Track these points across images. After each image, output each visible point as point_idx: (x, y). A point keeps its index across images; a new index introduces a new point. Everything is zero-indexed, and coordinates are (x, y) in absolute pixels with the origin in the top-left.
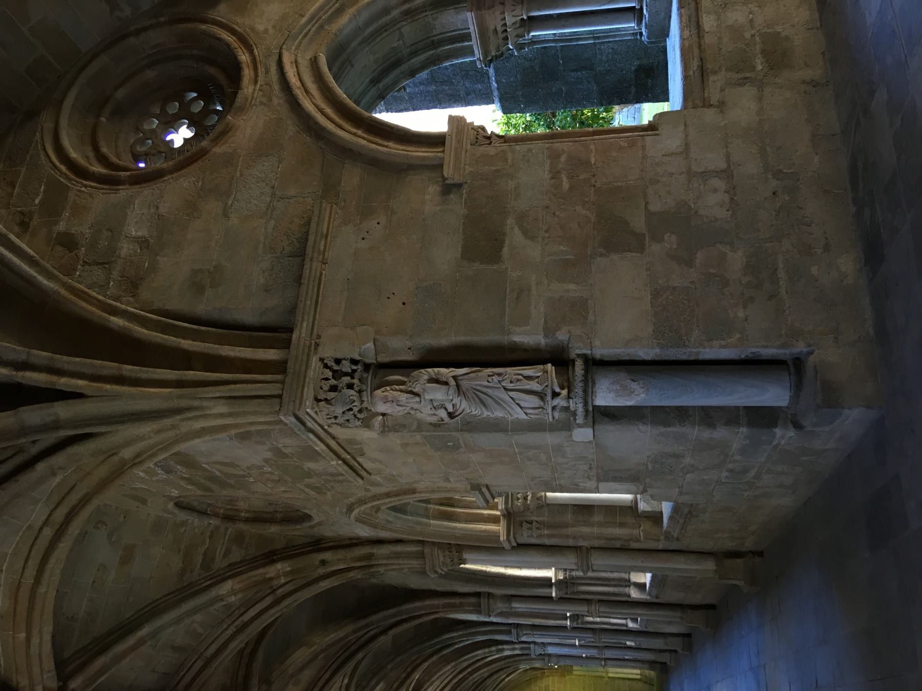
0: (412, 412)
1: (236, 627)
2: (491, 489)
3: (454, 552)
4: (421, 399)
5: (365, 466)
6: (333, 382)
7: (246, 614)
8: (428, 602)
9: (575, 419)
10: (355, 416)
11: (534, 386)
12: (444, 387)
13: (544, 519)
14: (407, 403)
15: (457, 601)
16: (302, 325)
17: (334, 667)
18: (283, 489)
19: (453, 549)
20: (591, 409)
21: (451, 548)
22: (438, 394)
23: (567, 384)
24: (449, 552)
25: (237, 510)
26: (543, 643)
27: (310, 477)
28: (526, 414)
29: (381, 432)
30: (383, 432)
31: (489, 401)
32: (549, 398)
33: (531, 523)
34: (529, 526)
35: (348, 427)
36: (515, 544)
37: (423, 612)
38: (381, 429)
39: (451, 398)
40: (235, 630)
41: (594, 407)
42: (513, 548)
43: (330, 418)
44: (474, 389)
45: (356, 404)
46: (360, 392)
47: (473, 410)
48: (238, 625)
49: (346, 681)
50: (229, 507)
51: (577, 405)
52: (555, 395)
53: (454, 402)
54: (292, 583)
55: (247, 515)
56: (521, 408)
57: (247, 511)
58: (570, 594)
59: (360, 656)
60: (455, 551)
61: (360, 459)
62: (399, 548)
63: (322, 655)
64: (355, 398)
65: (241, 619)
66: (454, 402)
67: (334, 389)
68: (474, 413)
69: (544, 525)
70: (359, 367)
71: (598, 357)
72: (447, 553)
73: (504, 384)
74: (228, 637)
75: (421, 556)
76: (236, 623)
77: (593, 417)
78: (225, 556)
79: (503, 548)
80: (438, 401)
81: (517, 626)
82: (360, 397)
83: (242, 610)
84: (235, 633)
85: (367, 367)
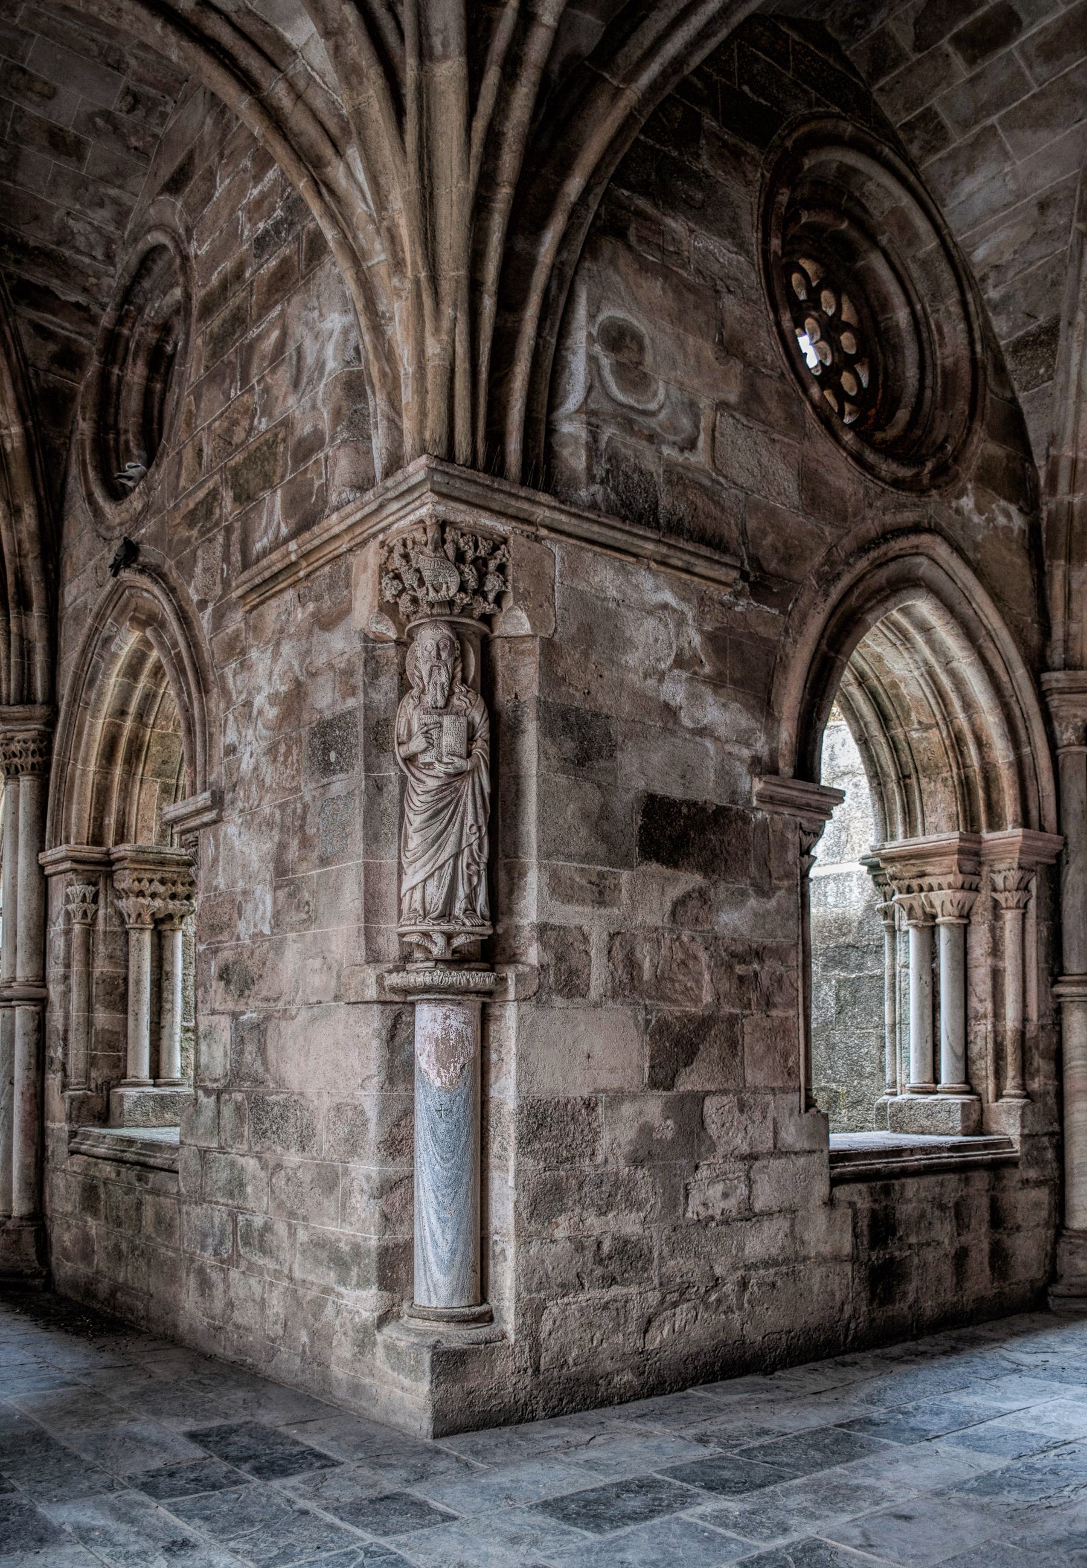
0: (415, 692)
2: (209, 831)
3: (30, 760)
5: (273, 603)
6: (470, 555)
9: (390, 972)
10: (404, 590)
11: (460, 906)
12: (463, 751)
13: (101, 926)
16: (562, 511)
18: (207, 450)
19: (38, 759)
20: (410, 998)
21: (41, 756)
22: (450, 737)
23: (458, 960)
24: (34, 752)
27: (237, 499)
28: (414, 888)
29: (366, 636)
30: (366, 638)
31: (438, 827)
32: (445, 927)
33: (95, 900)
34: (89, 899)
35: (381, 577)
36: (49, 870)
38: (371, 636)
39: (445, 760)
41: (413, 1004)
42: (41, 868)
43: (405, 545)
45: (432, 593)
46: (451, 603)
47: (422, 798)
50: (132, 345)
51: (419, 975)
52: (449, 937)
53: (437, 765)
55: (114, 379)
56: (425, 881)
57: (120, 379)
61: (290, 594)
62: (39, 658)
64: (443, 592)
66: (437, 765)
67: (460, 557)
68: (415, 798)
70: (489, 608)
71: (495, 1011)
72: (32, 746)
73: (466, 852)
75: (26, 697)
77: (392, 1003)
80: (439, 738)
82: (441, 604)
85: (487, 619)
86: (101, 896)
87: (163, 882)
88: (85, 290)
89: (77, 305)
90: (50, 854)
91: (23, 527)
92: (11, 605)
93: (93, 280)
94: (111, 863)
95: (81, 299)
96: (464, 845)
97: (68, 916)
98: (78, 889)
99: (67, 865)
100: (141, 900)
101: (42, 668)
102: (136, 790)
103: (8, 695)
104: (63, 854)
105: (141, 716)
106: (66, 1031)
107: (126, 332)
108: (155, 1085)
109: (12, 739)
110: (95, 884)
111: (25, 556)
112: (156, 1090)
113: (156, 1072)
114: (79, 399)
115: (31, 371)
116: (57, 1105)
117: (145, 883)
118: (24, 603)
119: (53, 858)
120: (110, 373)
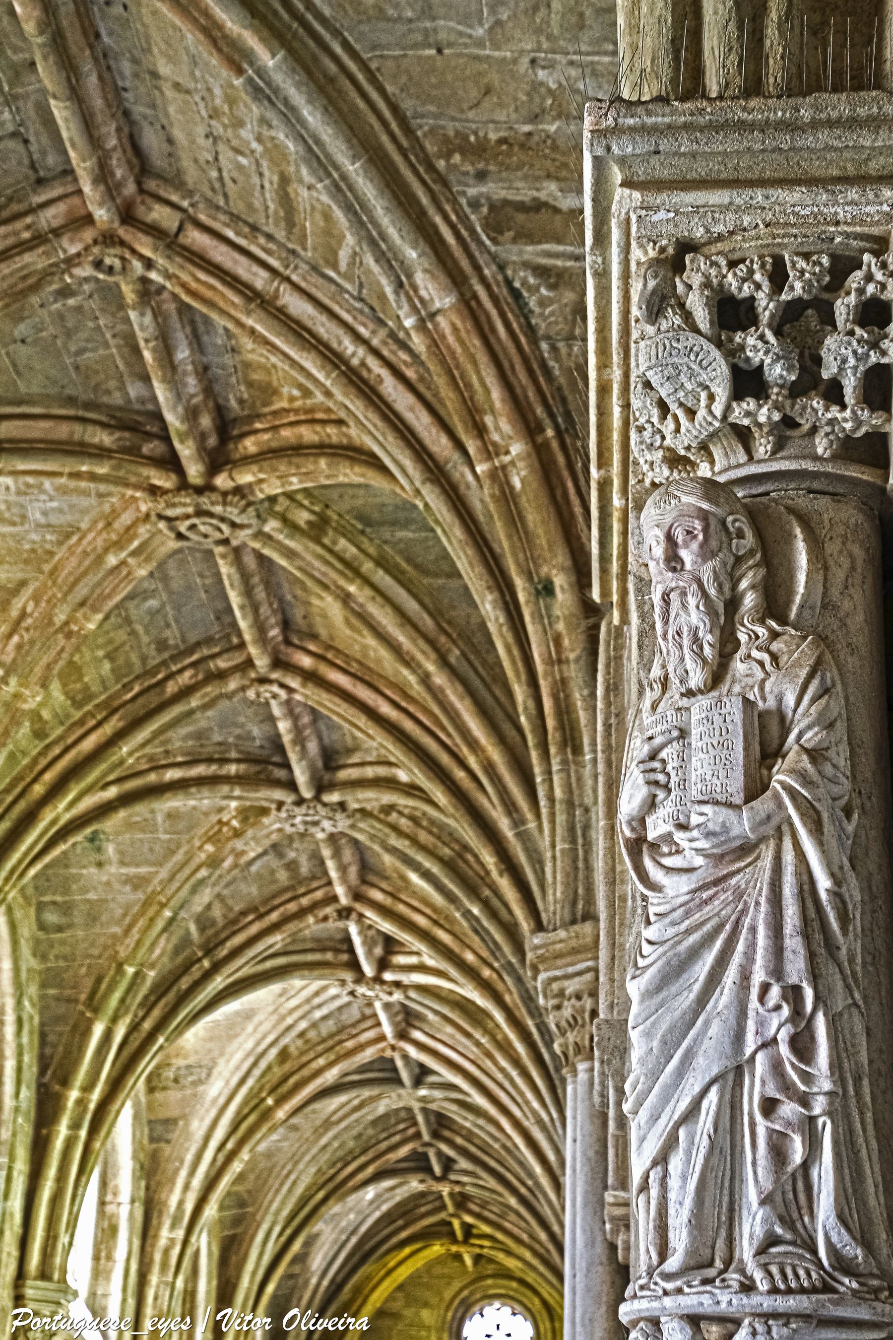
4: (701, 692)
7: (401, 387)
12: (736, 785)
14: (679, 634)
17: (408, 725)
40: (355, 362)
44: (737, 923)
48: (369, 370)
59: (440, 796)
65: (384, 373)
74: (335, 345)
76: (373, 363)
78: (542, 272)
84: (346, 363)
92: (553, 750)
96: (751, 1043)
115: (544, 346)
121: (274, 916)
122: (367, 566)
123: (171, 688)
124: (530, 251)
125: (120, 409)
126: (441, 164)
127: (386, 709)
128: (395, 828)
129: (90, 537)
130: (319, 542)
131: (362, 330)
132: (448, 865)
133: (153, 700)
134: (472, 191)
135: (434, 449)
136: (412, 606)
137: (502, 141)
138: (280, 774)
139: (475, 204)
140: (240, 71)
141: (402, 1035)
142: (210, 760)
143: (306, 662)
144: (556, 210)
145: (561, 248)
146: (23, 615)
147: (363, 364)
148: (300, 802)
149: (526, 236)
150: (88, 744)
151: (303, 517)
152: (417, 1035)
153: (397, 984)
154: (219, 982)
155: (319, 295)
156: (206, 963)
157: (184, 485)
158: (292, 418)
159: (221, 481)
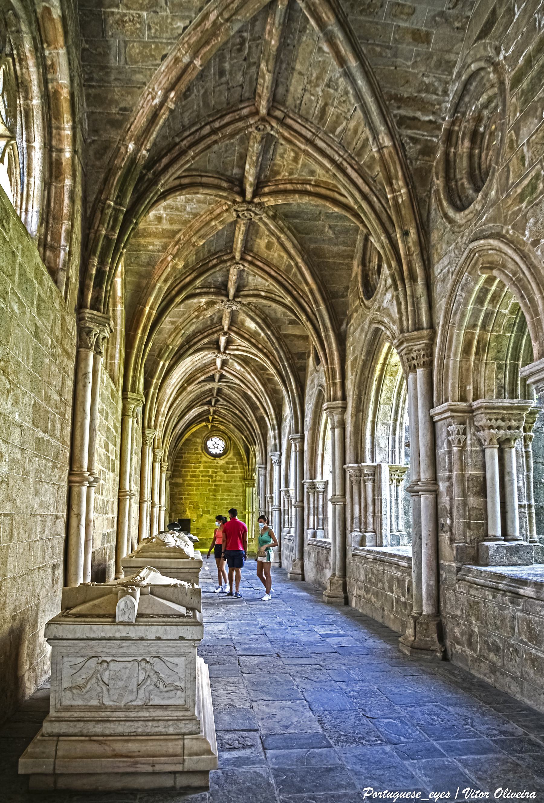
1: (341, 163)
7: (353, 171)
8: (336, 354)
15: (338, 381)
17: (280, 278)
19: (426, 359)
21: (427, 357)
24: (424, 355)
25: (457, 143)
26: (281, 461)
33: (464, 433)
36: (436, 418)
37: (327, 350)
40: (339, 162)
49: (263, 294)
54: (382, 209)
55: (452, 154)
57: (455, 154)
58: (350, 480)
59: (288, 300)
60: (425, 360)
63: (293, 264)
65: (348, 166)
69: (462, 447)
75: (418, 327)
78: (412, 139)
79: (432, 407)
81: (302, 438)
83: (356, 167)
86: (468, 430)
87: (503, 420)
88: (434, 113)
89: (430, 122)
90: (438, 409)
91: (410, 240)
93: (437, 107)
94: (472, 411)
95: (431, 118)
97: (449, 443)
98: (453, 428)
99: (448, 414)
100: (492, 431)
101: (426, 311)
102: (483, 369)
103: (408, 327)
104: (446, 408)
105: (484, 327)
106: (451, 509)
107: (456, 128)
108: (504, 540)
109: (412, 350)
110: (464, 423)
111: (412, 255)
112: (507, 544)
113: (504, 532)
114: (434, 170)
115: (408, 161)
116: (447, 551)
117: (493, 420)
118: (413, 278)
119: (439, 411)
120: (450, 152)
121: (206, 334)
122: (286, 229)
123: (210, 264)
124: (409, 132)
125: (229, 176)
126: (387, 103)
127: (273, 273)
128: (251, 309)
129: (204, 217)
130: (274, 220)
131: (341, 153)
132: (264, 320)
133: (205, 268)
134: (395, 112)
135: (364, 190)
136: (296, 242)
137: (408, 98)
138: (224, 292)
139: (395, 116)
140: (342, 67)
141: (222, 368)
142: (207, 287)
143: (249, 258)
144: (419, 120)
145: (419, 132)
146: (179, 240)
147: (341, 163)
148: (229, 300)
149: (409, 127)
150: (188, 280)
151: (271, 213)
152: (226, 368)
153: (229, 354)
154: (191, 351)
155: (327, 141)
156: (187, 346)
157: (244, 201)
158: (283, 182)
159: (256, 200)
